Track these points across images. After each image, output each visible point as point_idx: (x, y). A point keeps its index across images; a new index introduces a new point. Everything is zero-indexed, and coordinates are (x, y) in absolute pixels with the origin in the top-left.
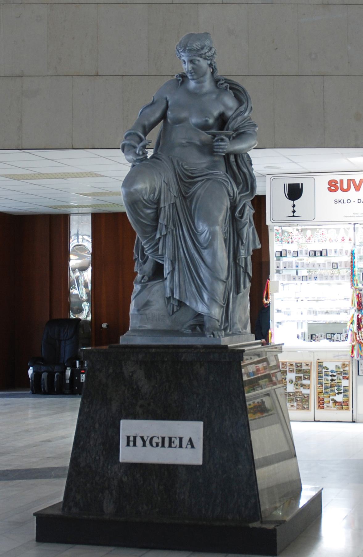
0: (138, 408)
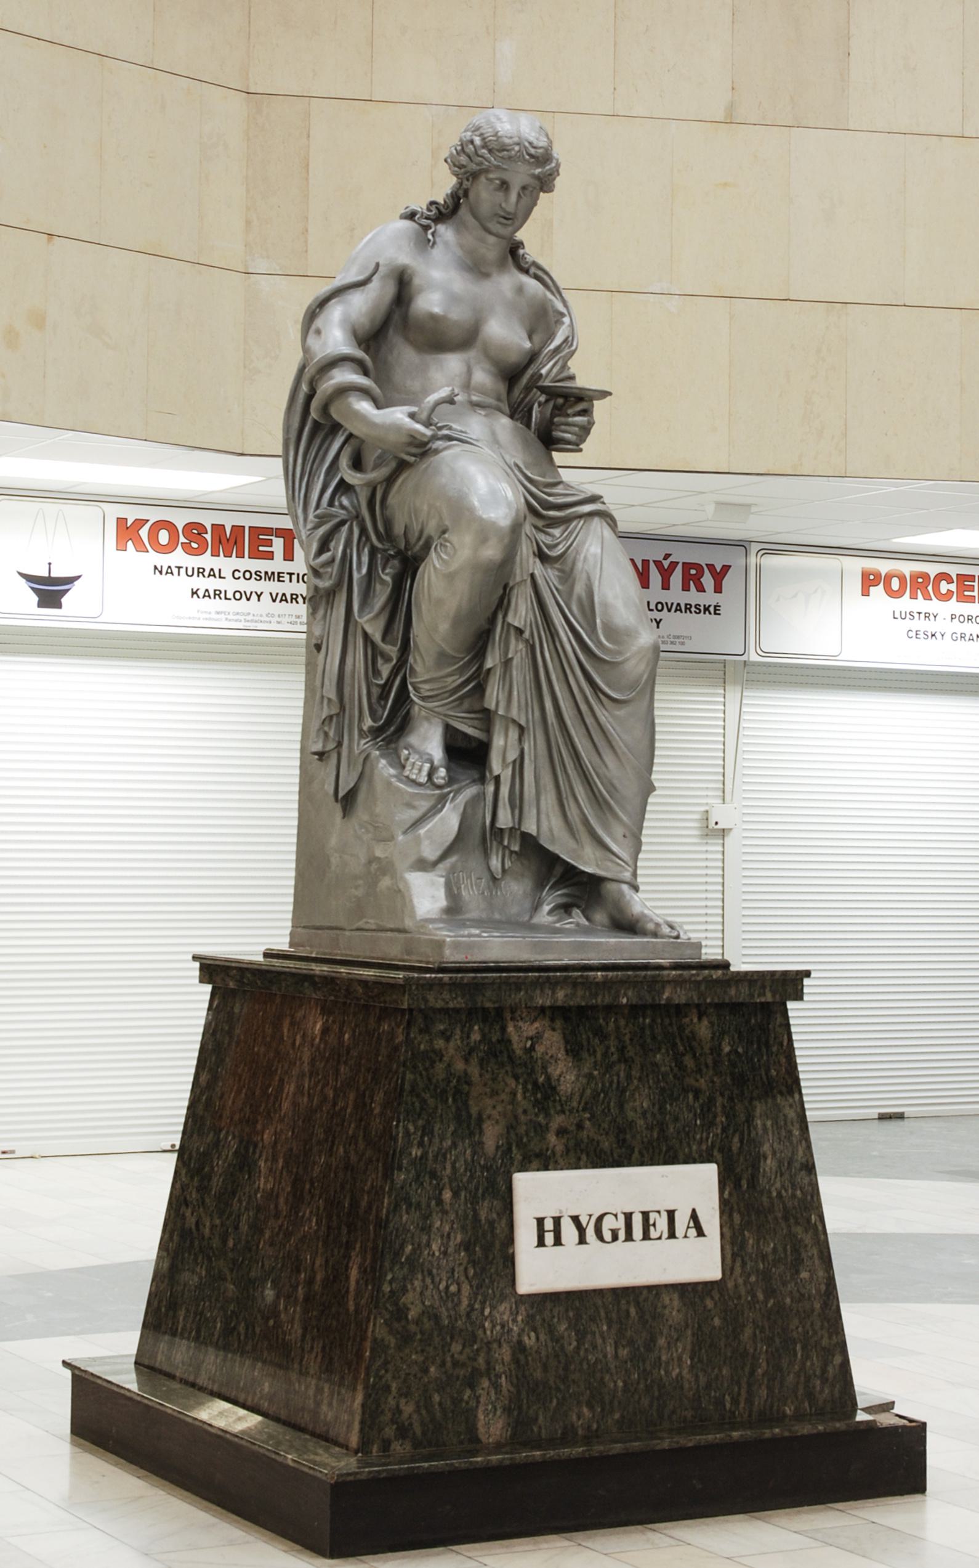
0: (552, 1138)
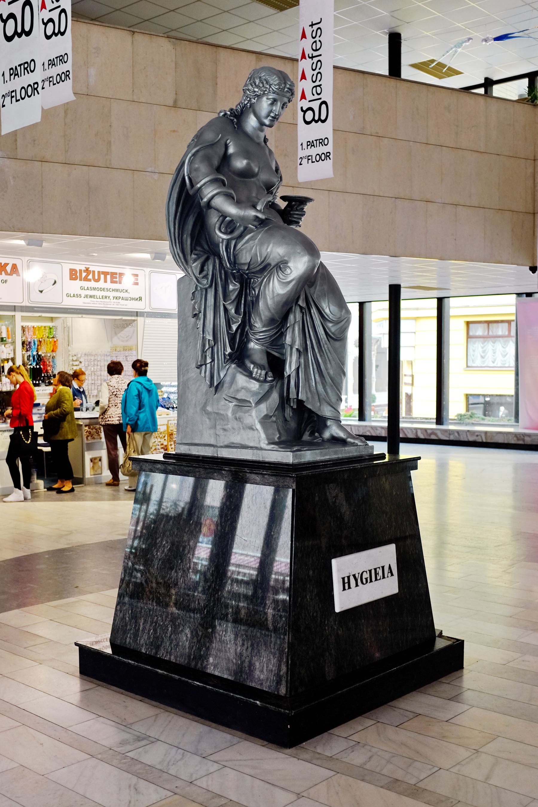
0: (343, 541)
